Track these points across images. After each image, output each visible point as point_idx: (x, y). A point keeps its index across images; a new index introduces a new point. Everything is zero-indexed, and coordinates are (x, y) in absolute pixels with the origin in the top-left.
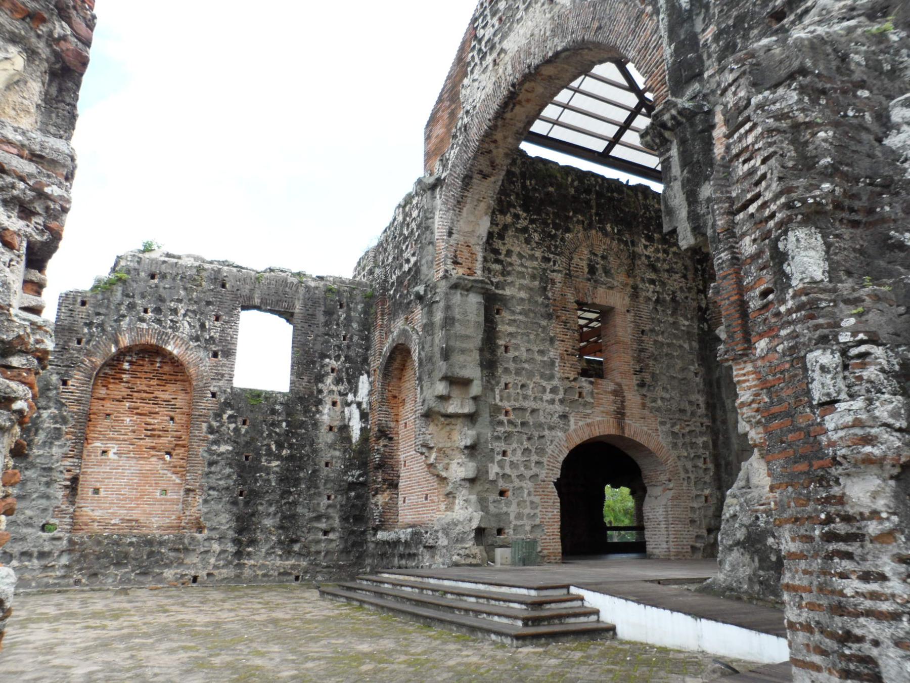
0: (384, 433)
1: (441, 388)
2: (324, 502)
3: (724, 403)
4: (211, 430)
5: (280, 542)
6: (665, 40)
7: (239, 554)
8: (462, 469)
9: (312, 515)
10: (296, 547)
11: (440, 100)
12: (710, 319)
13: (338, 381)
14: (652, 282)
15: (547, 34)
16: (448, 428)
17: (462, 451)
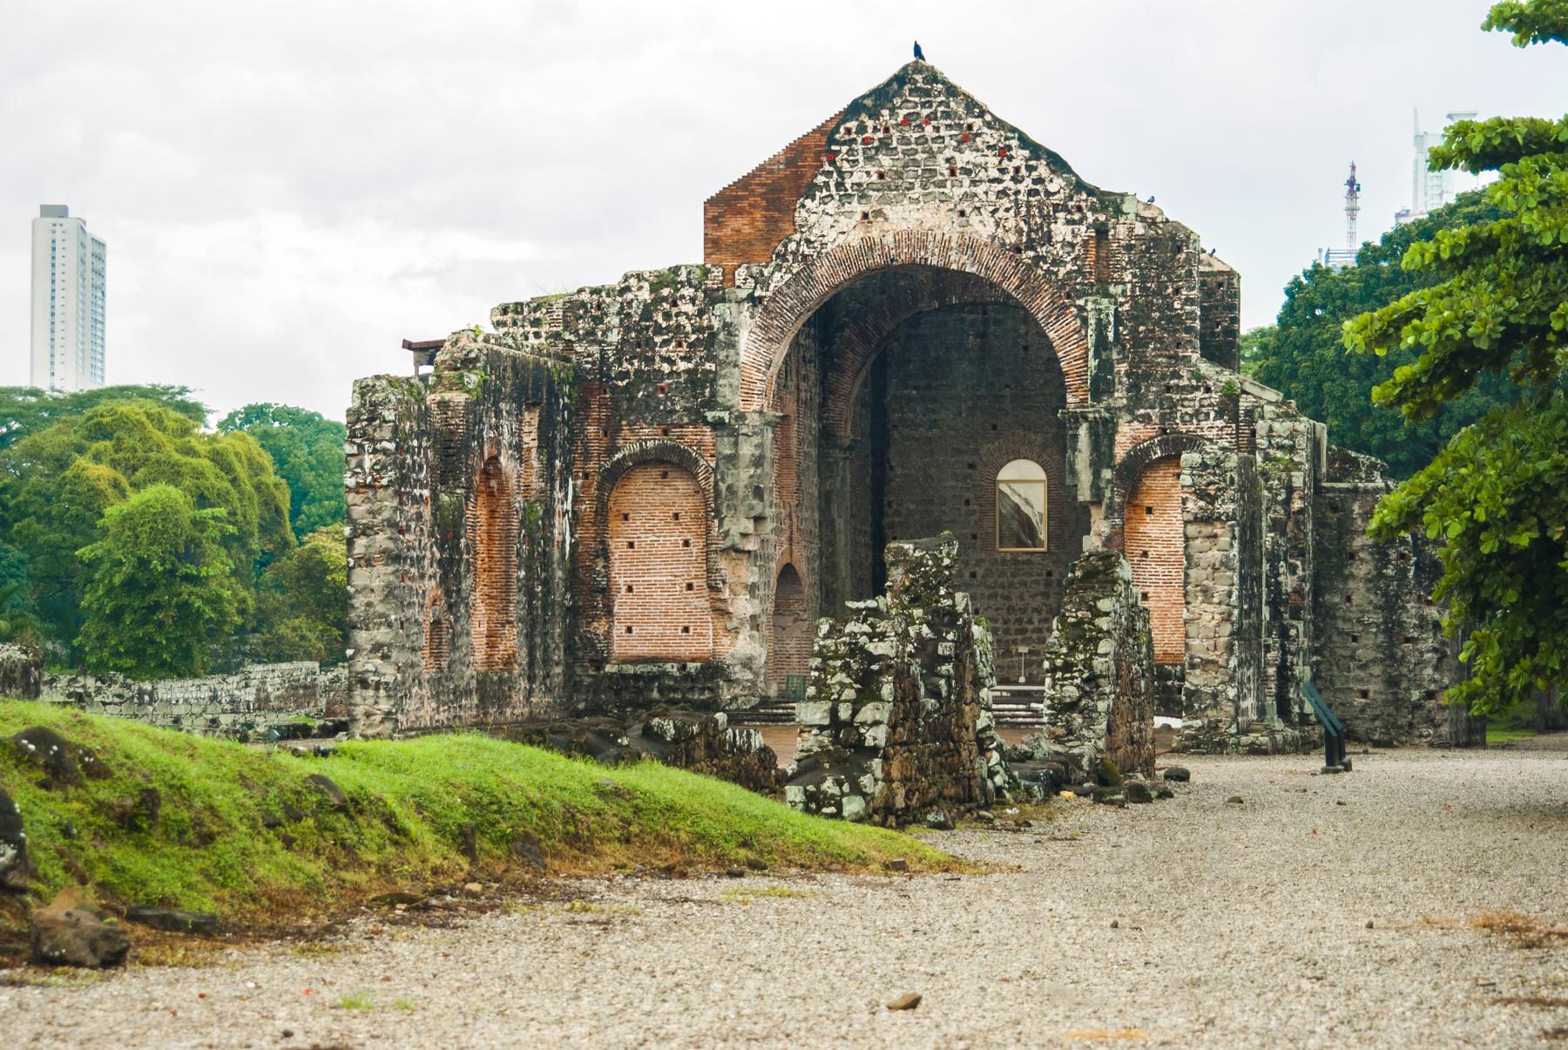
0: (605, 554)
1: (749, 526)
2: (558, 630)
3: (833, 521)
4: (518, 555)
5: (544, 679)
6: (1091, 354)
7: (530, 692)
8: (749, 606)
9: (553, 646)
10: (548, 682)
11: (745, 183)
12: (827, 419)
13: (561, 487)
14: (805, 378)
15: (953, 244)
16: (734, 563)
17: (746, 586)
